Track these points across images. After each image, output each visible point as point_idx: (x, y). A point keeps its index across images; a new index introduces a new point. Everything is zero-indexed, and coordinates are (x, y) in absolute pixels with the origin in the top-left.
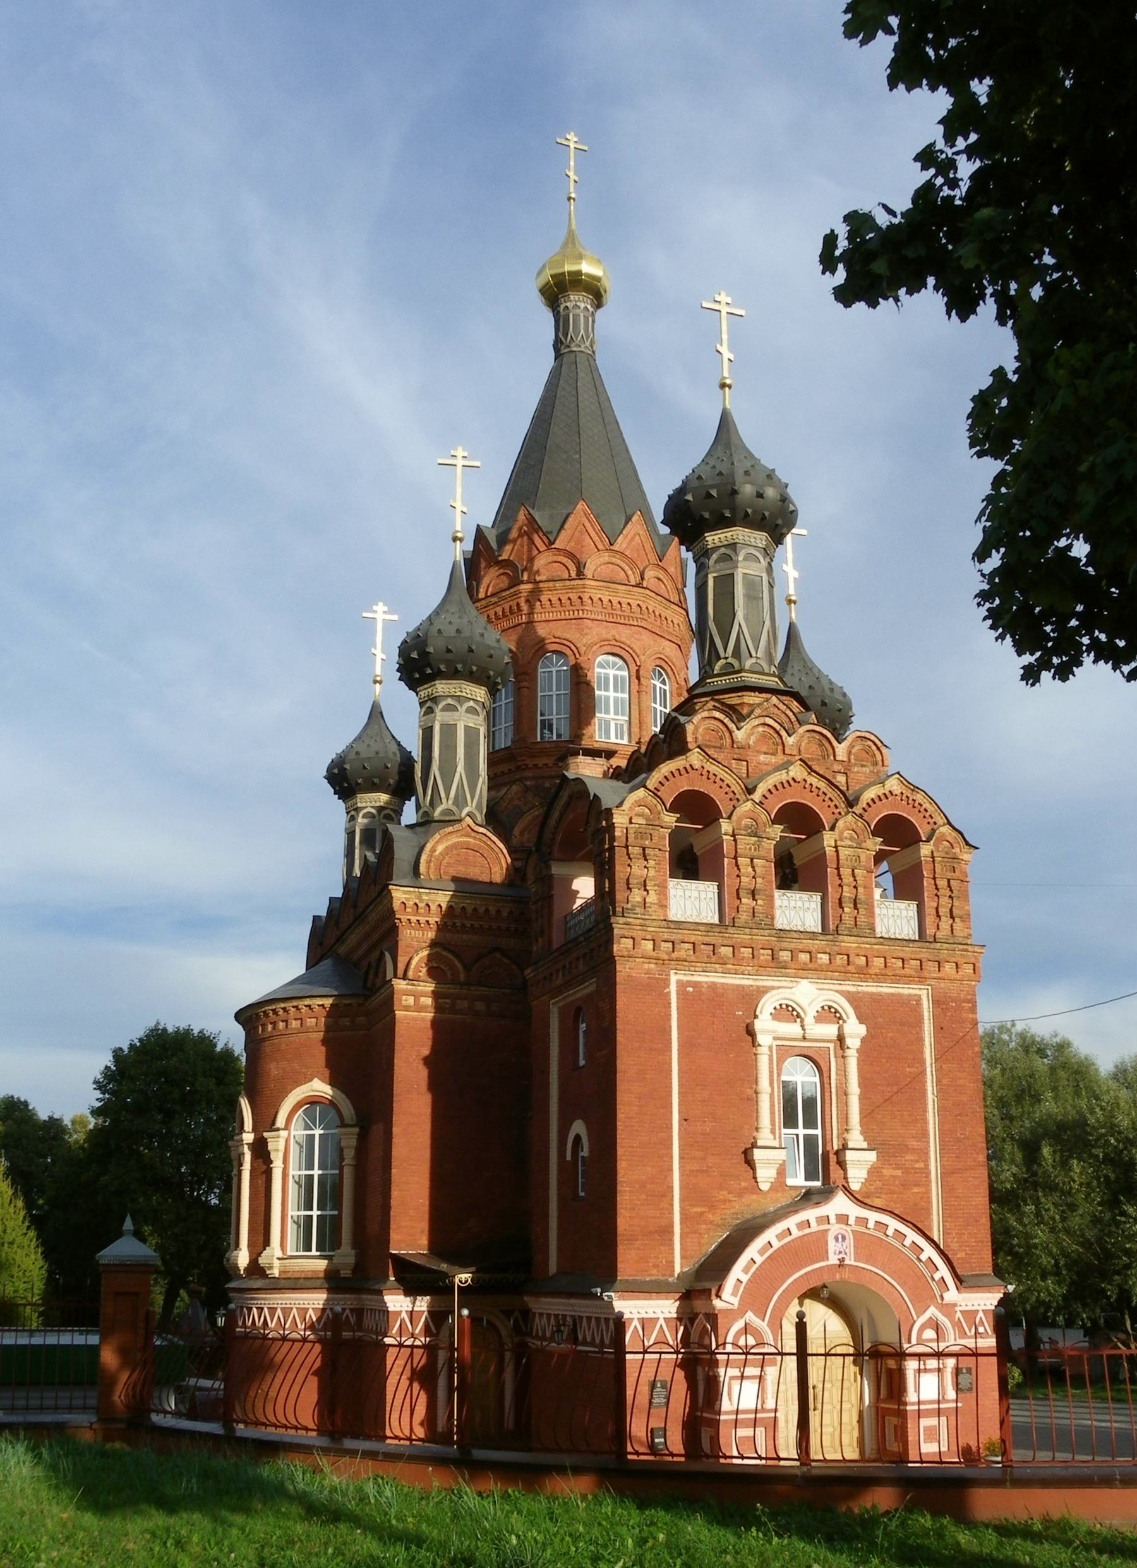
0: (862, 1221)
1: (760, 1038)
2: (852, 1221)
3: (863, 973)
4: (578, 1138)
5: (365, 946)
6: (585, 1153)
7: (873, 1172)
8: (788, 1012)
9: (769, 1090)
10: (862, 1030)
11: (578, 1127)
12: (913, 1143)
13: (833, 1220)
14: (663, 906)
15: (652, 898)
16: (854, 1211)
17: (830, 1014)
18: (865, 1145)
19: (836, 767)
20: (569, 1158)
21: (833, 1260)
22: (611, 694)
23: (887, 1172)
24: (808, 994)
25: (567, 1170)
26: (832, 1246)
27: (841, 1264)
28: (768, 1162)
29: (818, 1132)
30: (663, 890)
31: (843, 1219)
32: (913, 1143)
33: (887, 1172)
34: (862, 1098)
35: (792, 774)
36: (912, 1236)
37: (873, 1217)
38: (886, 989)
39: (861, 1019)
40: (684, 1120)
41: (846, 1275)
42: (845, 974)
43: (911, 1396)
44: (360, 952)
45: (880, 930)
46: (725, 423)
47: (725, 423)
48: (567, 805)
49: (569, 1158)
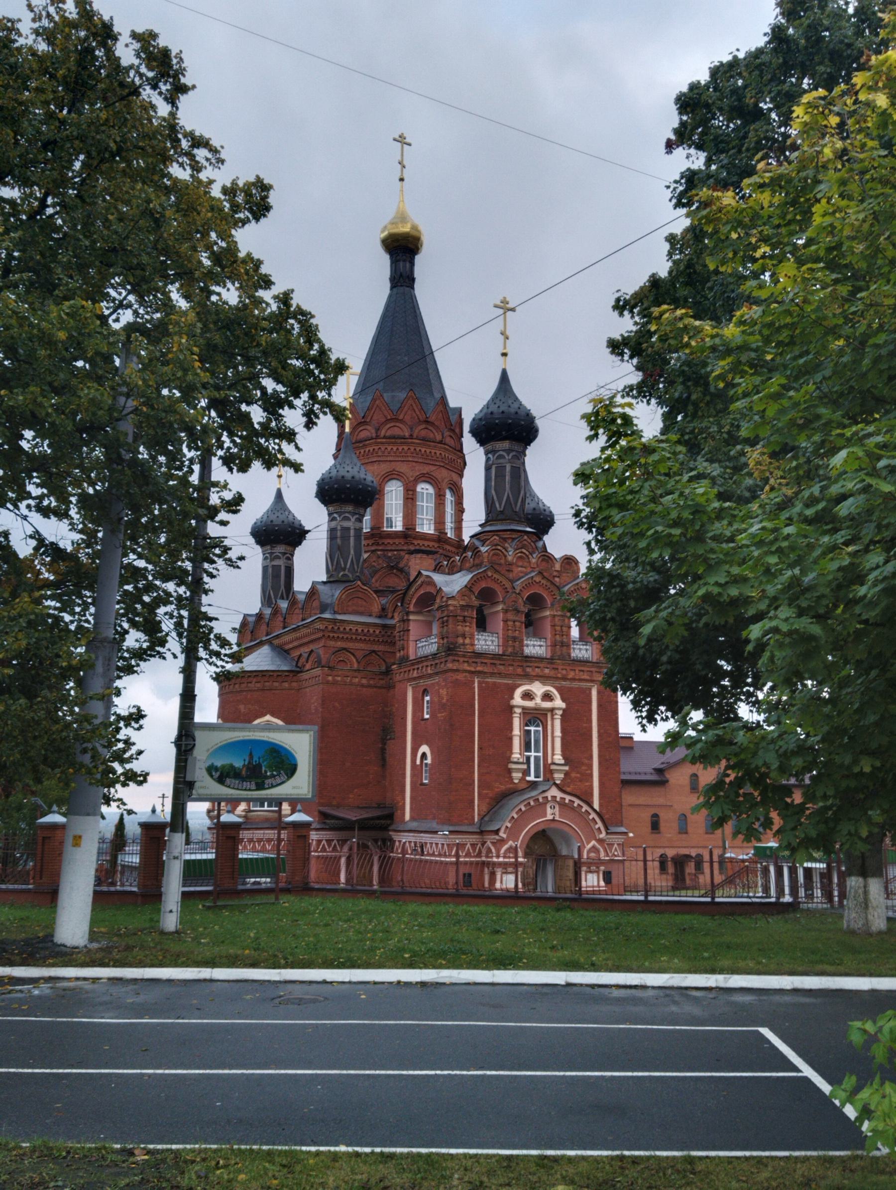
3: (564, 679)
4: (424, 755)
5: (296, 644)
6: (429, 761)
7: (567, 774)
8: (528, 696)
11: (424, 749)
12: (586, 761)
14: (473, 645)
15: (467, 641)
16: (559, 795)
17: (547, 697)
18: (563, 762)
20: (418, 762)
21: (549, 817)
22: (425, 504)
24: (538, 689)
25: (417, 771)
27: (553, 820)
28: (518, 770)
29: (541, 754)
30: (472, 637)
31: (554, 797)
32: (586, 761)
33: (573, 775)
34: (563, 739)
36: (585, 808)
37: (568, 798)
38: (576, 684)
39: (563, 700)
40: (480, 748)
41: (553, 825)
42: (557, 678)
43: (584, 884)
44: (291, 646)
45: (573, 655)
48: (421, 586)
49: (418, 762)
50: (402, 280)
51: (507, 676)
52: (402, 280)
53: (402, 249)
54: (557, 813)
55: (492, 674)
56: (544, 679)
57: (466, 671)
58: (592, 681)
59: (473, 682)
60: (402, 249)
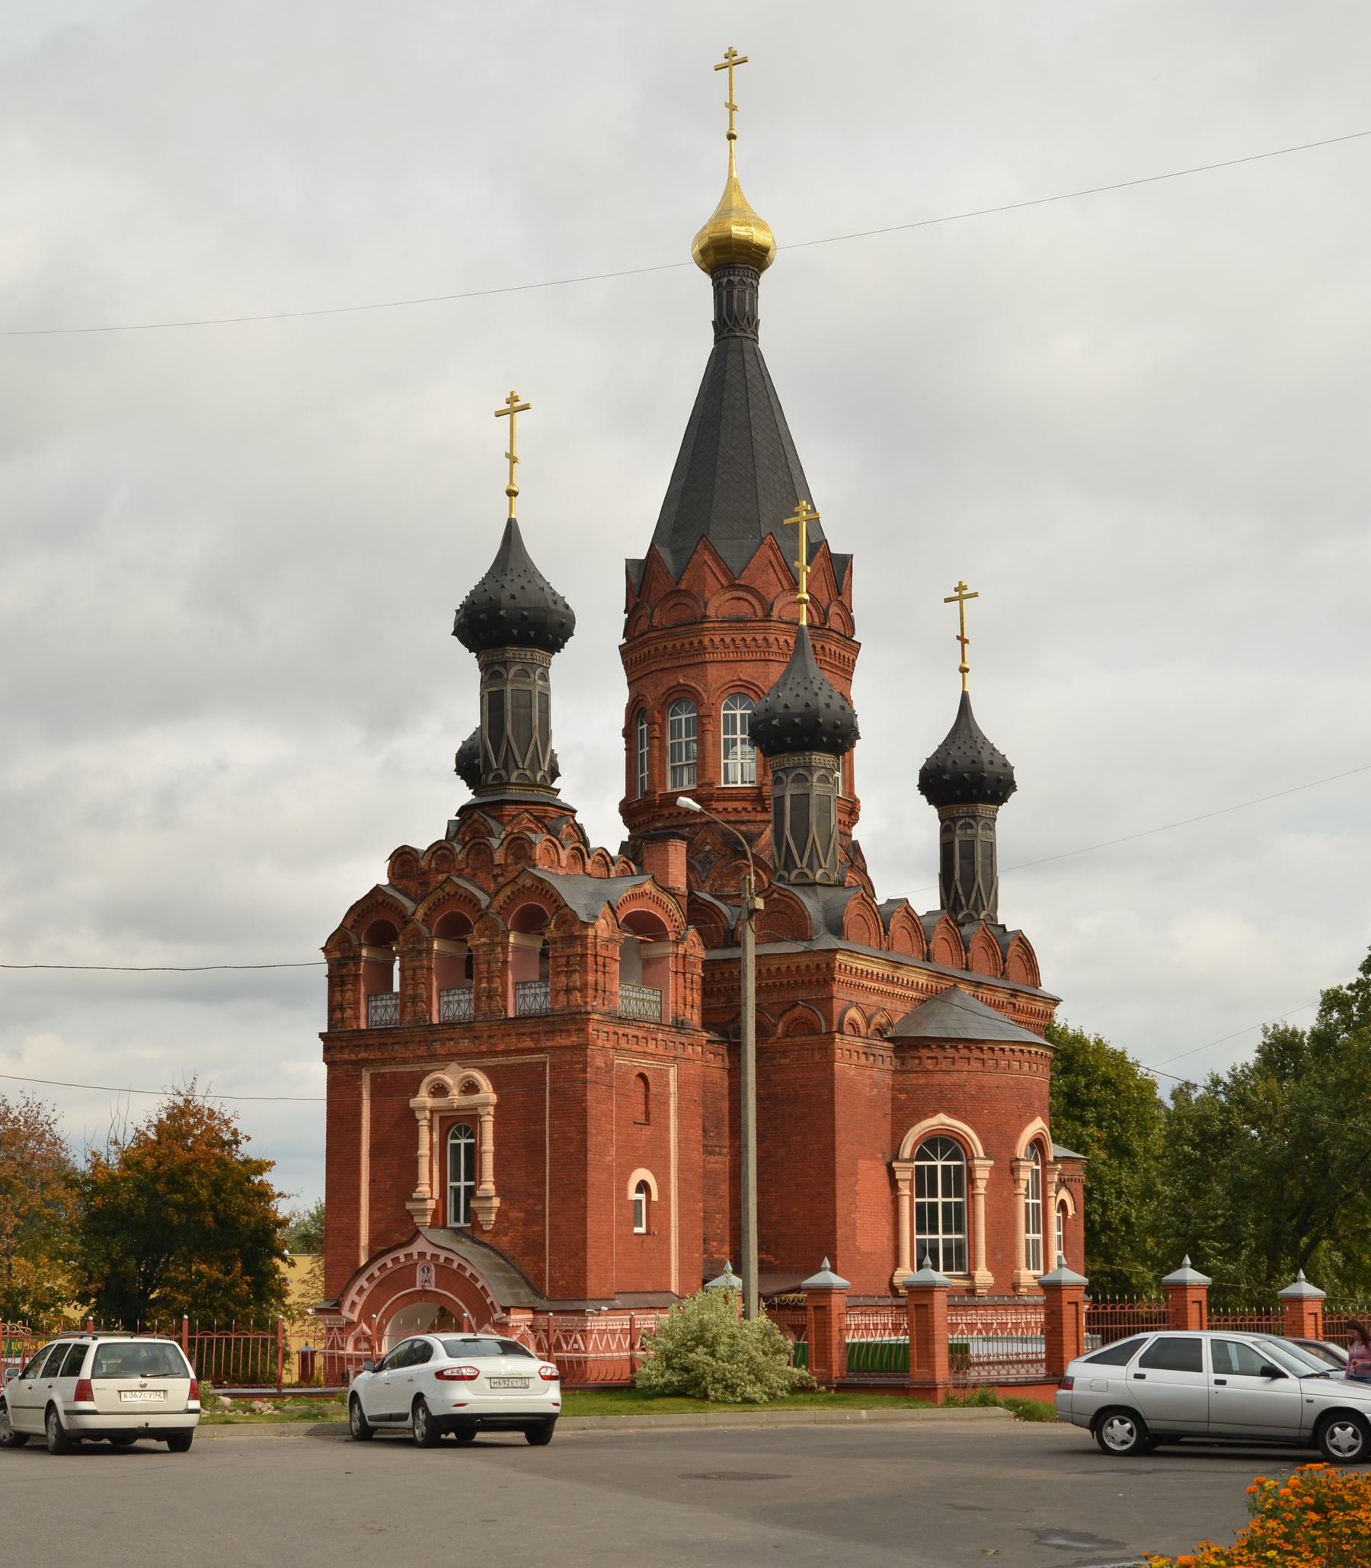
0: (435, 1257)
1: (419, 1115)
2: (428, 1257)
3: (494, 1054)
8: (440, 1090)
9: (427, 1152)
10: (493, 1098)
12: (536, 1190)
13: (415, 1257)
15: (349, 1013)
16: (430, 1251)
19: (496, 871)
21: (418, 1288)
23: (513, 1214)
24: (451, 1076)
26: (419, 1276)
29: (450, 1184)
31: (422, 1255)
33: (513, 1214)
34: (496, 1155)
35: (447, 889)
42: (481, 1054)
46: (511, 534)
47: (511, 534)
50: (734, 323)
51: (405, 1061)
52: (734, 323)
53: (733, 265)
54: (433, 1280)
55: (384, 1062)
56: (463, 1057)
57: (347, 1062)
58: (541, 1050)
59: (359, 1077)
60: (733, 265)
